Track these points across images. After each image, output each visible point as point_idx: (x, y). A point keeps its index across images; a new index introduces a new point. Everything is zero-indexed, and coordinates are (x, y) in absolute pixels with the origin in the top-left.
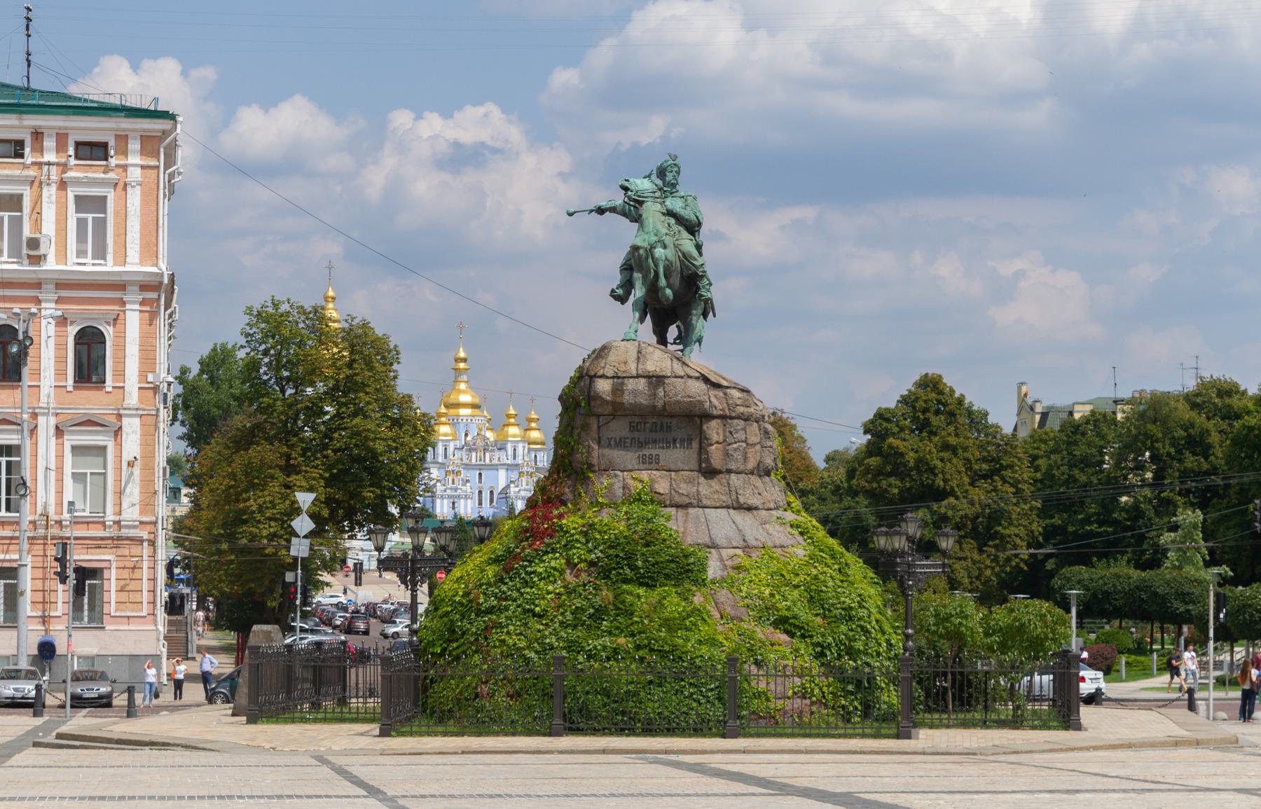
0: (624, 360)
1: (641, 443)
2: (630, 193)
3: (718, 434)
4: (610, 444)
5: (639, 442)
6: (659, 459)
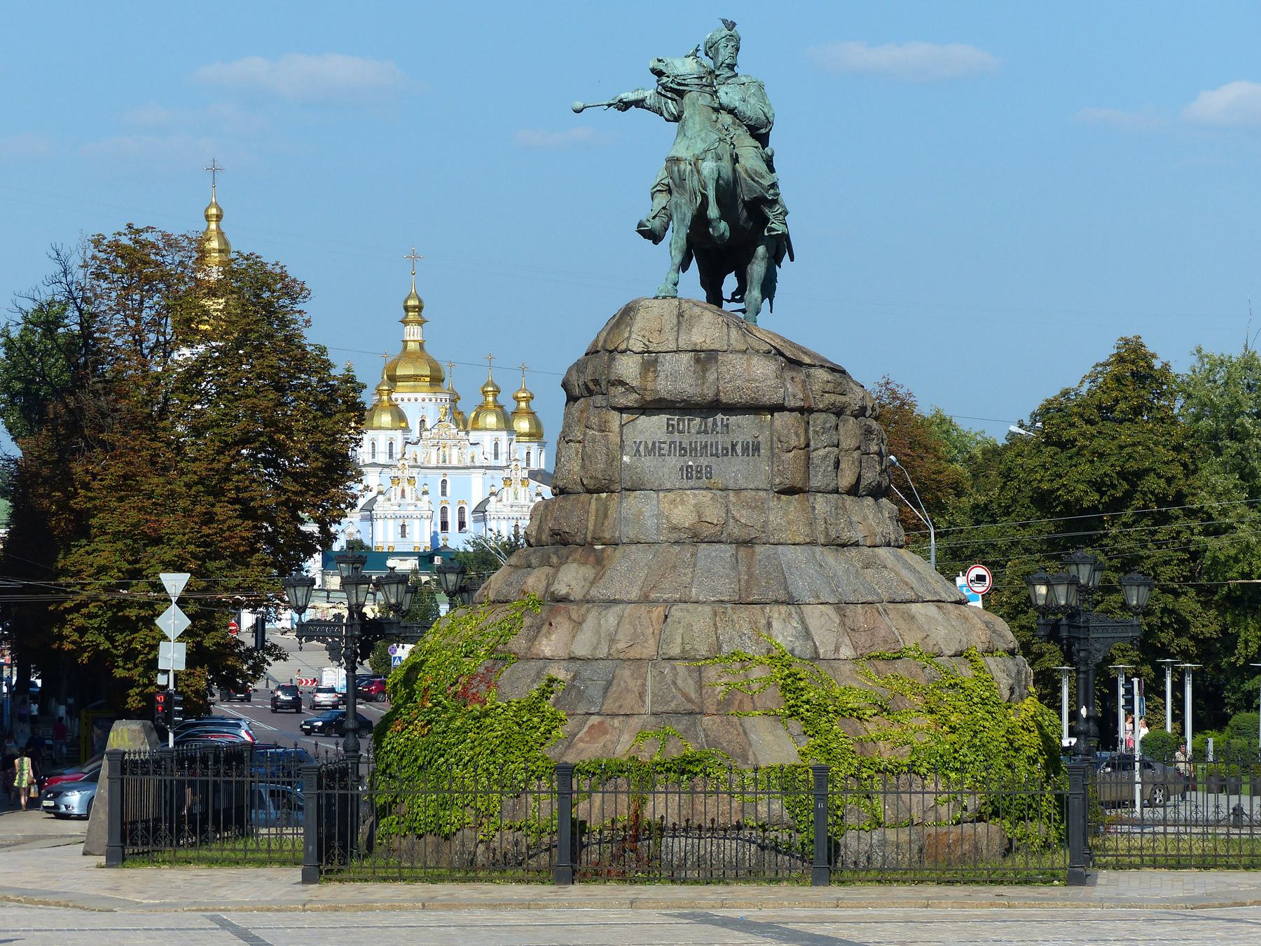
0: (656, 326)
1: (684, 449)
2: (664, 80)
3: (797, 435)
4: (638, 450)
5: (682, 448)
6: (711, 474)
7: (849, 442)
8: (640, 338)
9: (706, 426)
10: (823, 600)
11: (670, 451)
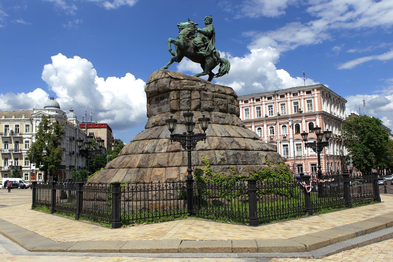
3: (174, 96)
6: (161, 109)
10: (167, 137)
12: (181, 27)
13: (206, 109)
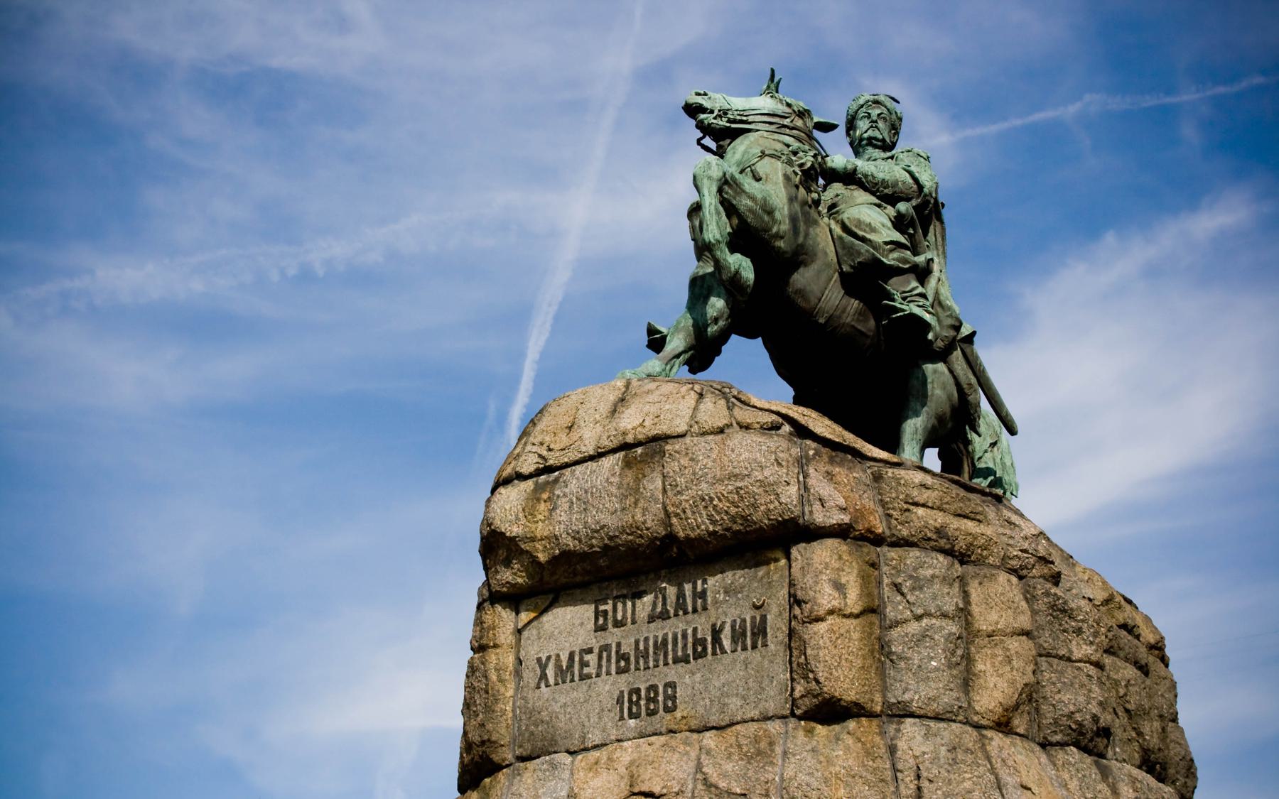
0: (567, 421)
1: (625, 657)
2: (702, 116)
3: (839, 587)
4: (544, 676)
5: (623, 657)
6: (674, 698)
7: (993, 616)
8: (535, 449)
9: (664, 604)
11: (600, 666)
12: (715, 118)
13: (1080, 725)
